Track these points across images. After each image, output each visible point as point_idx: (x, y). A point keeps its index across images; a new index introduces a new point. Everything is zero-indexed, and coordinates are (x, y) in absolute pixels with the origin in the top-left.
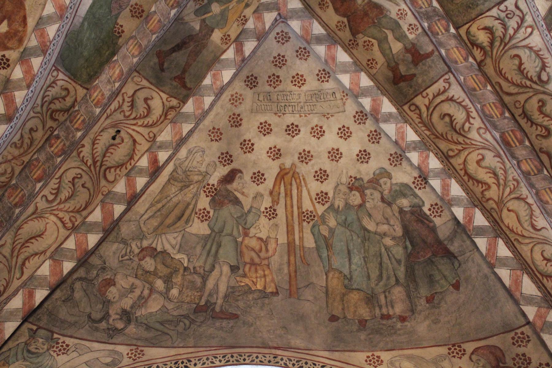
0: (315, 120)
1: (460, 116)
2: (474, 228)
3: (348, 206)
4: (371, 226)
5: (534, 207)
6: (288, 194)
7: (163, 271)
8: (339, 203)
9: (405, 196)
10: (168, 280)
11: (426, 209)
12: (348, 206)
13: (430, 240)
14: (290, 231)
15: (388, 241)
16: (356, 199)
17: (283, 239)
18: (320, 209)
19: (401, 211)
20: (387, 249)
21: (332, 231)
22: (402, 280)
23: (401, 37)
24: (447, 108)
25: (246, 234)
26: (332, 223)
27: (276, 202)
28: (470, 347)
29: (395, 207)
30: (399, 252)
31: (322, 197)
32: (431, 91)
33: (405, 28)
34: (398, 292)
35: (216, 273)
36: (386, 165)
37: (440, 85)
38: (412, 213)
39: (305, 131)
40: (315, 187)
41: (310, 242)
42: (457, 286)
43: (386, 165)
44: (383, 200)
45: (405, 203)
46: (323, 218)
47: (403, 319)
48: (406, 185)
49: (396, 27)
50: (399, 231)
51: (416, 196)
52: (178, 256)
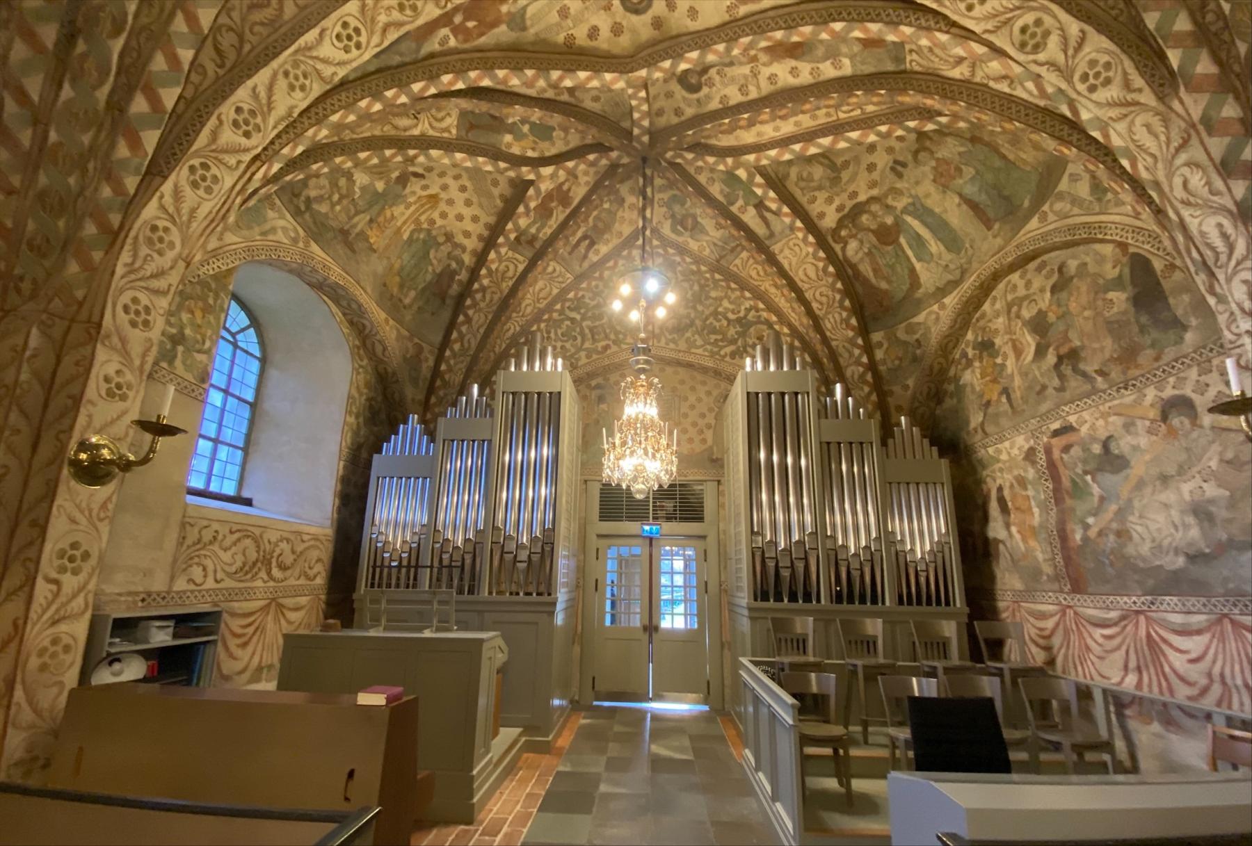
0: (475, 200)
1: (510, 274)
3: (435, 238)
4: (431, 256)
6: (422, 206)
7: (344, 191)
8: (434, 233)
10: (342, 197)
11: (457, 278)
12: (435, 238)
14: (405, 223)
15: (430, 269)
16: (441, 239)
17: (399, 224)
18: (425, 226)
19: (449, 265)
20: (427, 271)
21: (418, 239)
23: (539, 230)
24: (512, 267)
25: (391, 206)
26: (422, 236)
27: (415, 203)
30: (429, 277)
31: (432, 222)
32: (517, 256)
34: (412, 294)
35: (362, 216)
36: (469, 250)
37: (521, 258)
39: (466, 195)
40: (436, 215)
41: (405, 237)
42: (433, 314)
43: (469, 250)
44: (449, 253)
45: (454, 265)
46: (421, 230)
47: (405, 307)
49: (543, 226)
50: (438, 271)
52: (357, 190)
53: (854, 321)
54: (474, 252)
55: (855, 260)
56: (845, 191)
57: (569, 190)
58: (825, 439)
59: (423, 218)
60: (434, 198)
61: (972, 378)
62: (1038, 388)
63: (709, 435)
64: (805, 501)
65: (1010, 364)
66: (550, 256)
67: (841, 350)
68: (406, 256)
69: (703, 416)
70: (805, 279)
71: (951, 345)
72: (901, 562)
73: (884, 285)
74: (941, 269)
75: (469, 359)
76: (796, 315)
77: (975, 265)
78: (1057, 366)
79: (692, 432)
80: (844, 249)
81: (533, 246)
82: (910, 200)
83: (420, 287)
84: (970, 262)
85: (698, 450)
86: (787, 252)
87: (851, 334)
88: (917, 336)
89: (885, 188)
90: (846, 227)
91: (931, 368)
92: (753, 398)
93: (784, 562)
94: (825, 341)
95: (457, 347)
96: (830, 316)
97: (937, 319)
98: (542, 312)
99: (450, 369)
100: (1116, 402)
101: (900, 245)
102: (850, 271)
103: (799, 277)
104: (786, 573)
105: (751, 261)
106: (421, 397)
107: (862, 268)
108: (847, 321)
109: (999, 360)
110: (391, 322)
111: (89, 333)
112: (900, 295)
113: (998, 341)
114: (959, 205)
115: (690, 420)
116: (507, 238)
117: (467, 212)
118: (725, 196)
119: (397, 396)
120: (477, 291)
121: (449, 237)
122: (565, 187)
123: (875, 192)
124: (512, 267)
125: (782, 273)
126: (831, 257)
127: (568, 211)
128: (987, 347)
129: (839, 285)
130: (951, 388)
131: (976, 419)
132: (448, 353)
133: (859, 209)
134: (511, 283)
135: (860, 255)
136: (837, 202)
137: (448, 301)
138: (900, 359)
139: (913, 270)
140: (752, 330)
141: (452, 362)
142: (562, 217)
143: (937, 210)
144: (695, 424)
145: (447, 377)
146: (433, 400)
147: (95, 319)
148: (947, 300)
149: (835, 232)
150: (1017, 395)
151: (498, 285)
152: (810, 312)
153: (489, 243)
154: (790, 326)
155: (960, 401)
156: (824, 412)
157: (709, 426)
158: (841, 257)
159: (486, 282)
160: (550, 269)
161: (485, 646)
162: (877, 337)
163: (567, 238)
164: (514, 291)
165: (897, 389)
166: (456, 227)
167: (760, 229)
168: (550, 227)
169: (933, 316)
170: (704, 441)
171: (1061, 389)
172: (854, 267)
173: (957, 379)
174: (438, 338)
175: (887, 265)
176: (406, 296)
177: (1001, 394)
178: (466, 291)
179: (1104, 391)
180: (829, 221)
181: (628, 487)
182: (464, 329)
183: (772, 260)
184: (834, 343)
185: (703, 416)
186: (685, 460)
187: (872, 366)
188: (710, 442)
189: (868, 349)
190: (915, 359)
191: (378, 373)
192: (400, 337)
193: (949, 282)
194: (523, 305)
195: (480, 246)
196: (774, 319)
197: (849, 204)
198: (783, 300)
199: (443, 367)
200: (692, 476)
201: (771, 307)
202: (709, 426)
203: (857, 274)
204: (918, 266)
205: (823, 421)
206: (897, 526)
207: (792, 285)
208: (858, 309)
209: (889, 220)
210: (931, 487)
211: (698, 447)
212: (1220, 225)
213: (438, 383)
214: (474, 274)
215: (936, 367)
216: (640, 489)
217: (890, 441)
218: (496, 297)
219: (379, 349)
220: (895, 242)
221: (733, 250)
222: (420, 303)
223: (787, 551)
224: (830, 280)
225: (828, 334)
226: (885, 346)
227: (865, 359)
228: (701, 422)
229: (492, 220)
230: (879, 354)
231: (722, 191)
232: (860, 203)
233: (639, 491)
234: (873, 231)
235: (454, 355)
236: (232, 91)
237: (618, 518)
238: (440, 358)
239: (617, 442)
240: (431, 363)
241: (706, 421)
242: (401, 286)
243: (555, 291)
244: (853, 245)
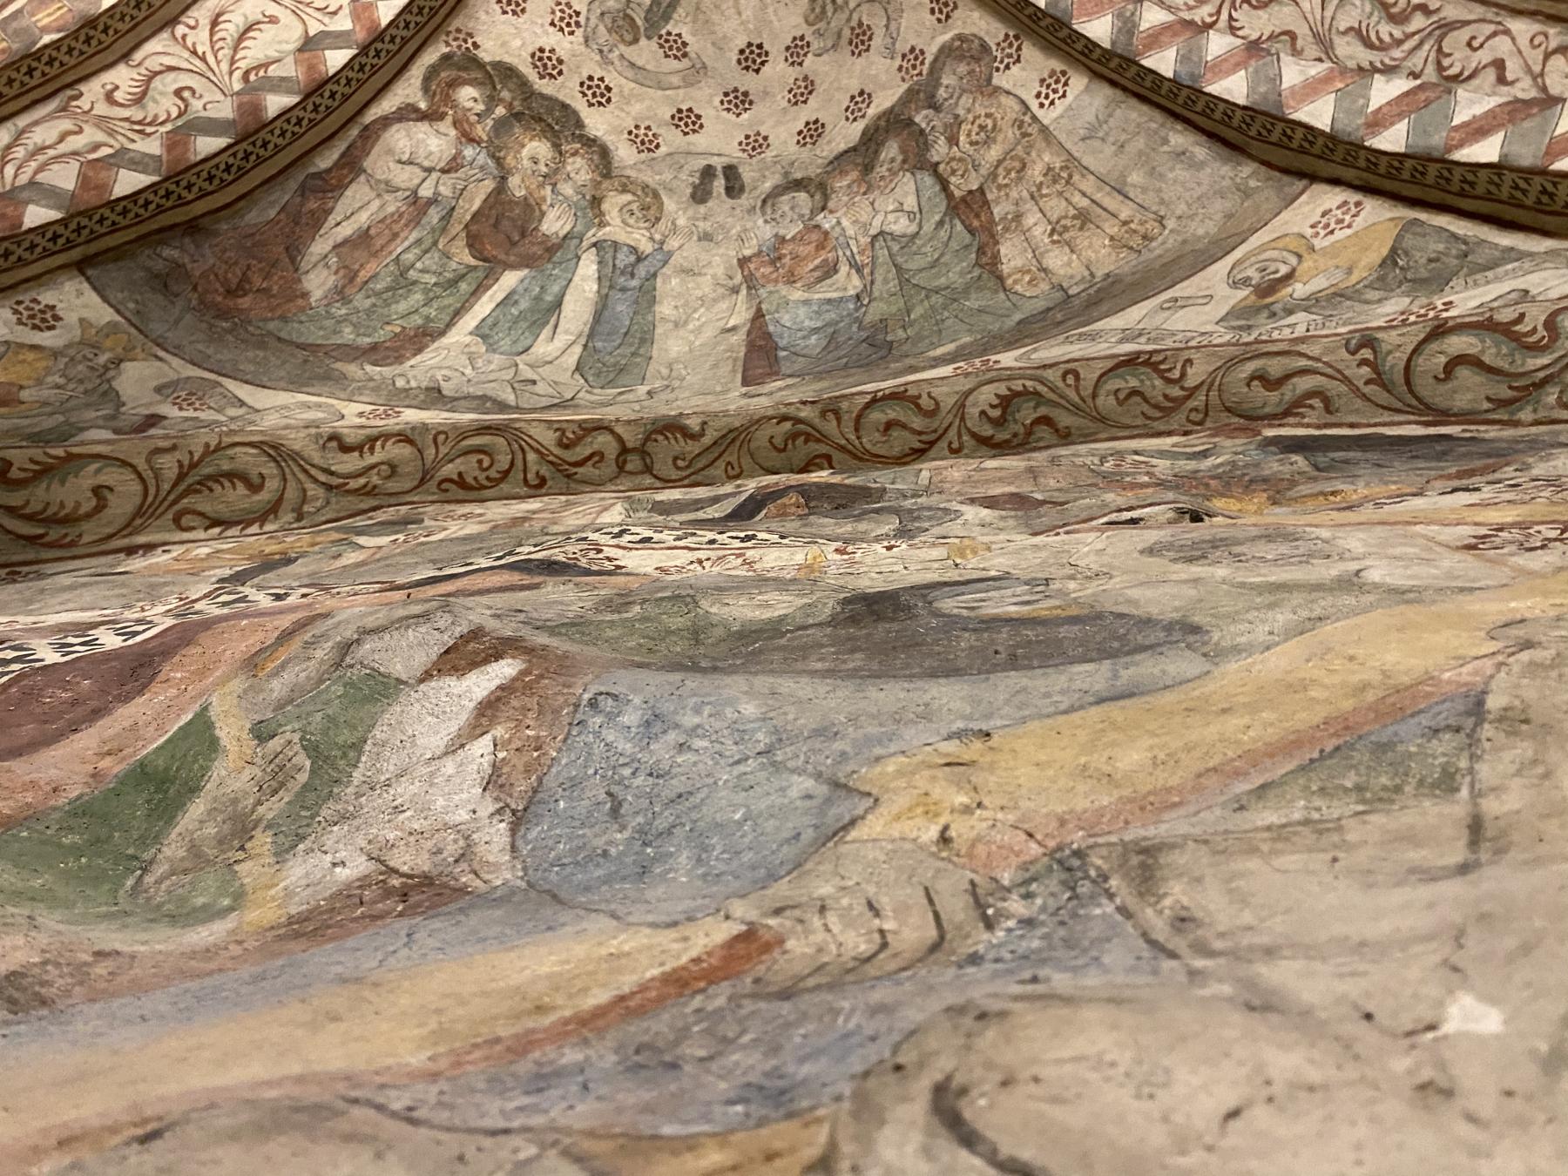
55: (378, 163)
70: (229, 29)
73: (318, 283)
80: (408, 113)
82: (646, 247)
90: (492, 101)
102: (325, 161)
107: (357, 193)
123: (624, 154)
135: (405, 177)
136: (564, 45)
149: (467, 65)
158: (374, 113)
172: (351, 165)
197: (566, 90)
203: (331, 185)
209: (555, 223)
220: (492, 268)
232: (579, 124)
244: (434, 142)
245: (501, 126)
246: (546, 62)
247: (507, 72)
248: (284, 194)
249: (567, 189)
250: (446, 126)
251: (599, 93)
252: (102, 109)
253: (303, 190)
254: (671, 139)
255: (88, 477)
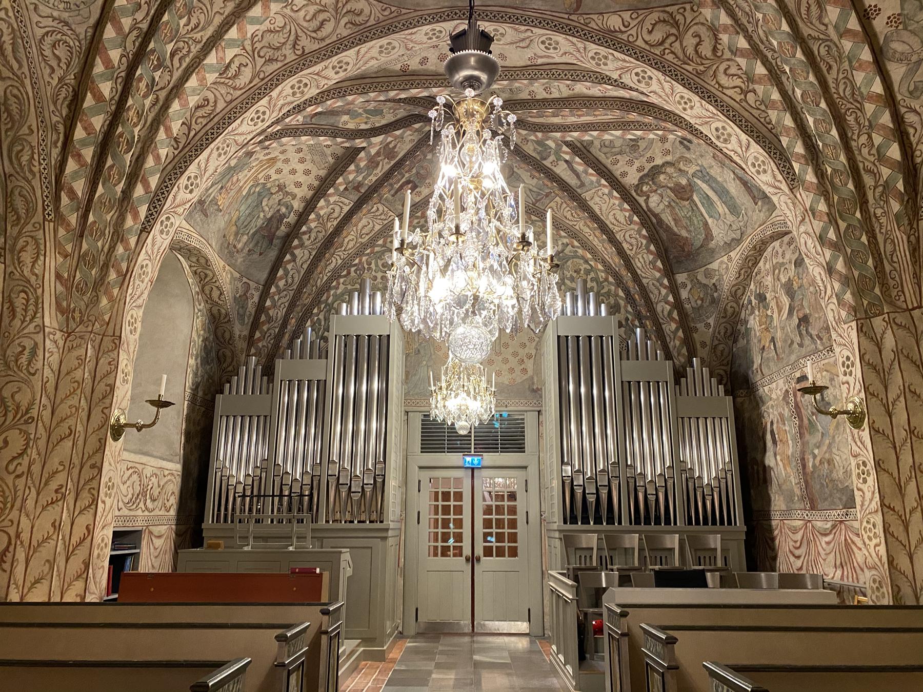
0: (308, 157)
1: (336, 215)
2: (293, 252)
4: (264, 204)
5: (310, 260)
8: (269, 185)
9: (287, 208)
11: (285, 220)
13: (273, 230)
15: (262, 215)
19: (278, 211)
20: (258, 217)
22: (250, 234)
23: (365, 179)
24: (337, 209)
26: (257, 190)
28: (245, 280)
29: (279, 207)
30: (260, 222)
33: (370, 178)
36: (298, 197)
37: (347, 201)
38: (280, 215)
40: (272, 172)
45: (284, 210)
46: (258, 184)
48: (293, 208)
50: (269, 216)
51: (290, 213)
53: (659, 264)
54: (303, 199)
55: (657, 210)
56: (643, 156)
57: (395, 146)
58: (625, 379)
59: (260, 176)
60: (274, 160)
61: (754, 322)
62: (789, 342)
63: (529, 365)
64: (609, 431)
65: (775, 316)
66: (375, 200)
67: (652, 287)
68: (243, 208)
69: (524, 345)
70: (615, 222)
71: (740, 292)
72: (691, 485)
73: (684, 233)
74: (727, 228)
75: (292, 293)
76: (609, 253)
77: (749, 231)
78: (799, 326)
79: (513, 362)
80: (646, 201)
81: (359, 191)
82: (698, 168)
83: (251, 232)
84: (746, 226)
85: (519, 380)
86: (597, 199)
87: (658, 275)
88: (714, 281)
89: (678, 155)
90: (647, 184)
91: (725, 310)
92: (563, 341)
93: (591, 489)
94: (636, 278)
95: (281, 283)
96: (640, 256)
97: (727, 268)
98: (364, 246)
99: (274, 306)
100: (826, 361)
101: (693, 201)
102: (654, 220)
103: (609, 220)
104: (592, 499)
105: (564, 205)
106: (246, 333)
107: (663, 217)
108: (653, 263)
109: (769, 313)
110: (227, 268)
111: (115, 343)
112: (698, 244)
113: (768, 296)
114: (734, 179)
115: (511, 350)
116: (337, 189)
117: (300, 168)
118: (538, 153)
119: (227, 335)
120: (305, 233)
121: (281, 188)
122: (391, 146)
123: (669, 158)
124: (337, 209)
125: (594, 217)
126: (636, 208)
127: (393, 163)
128: (762, 298)
129: (644, 232)
130: (743, 329)
131: (757, 361)
132: (273, 289)
133: (655, 172)
134: (335, 223)
135: (662, 206)
136: (637, 164)
137: (276, 241)
138: (702, 300)
139: (706, 224)
140: (569, 263)
141: (276, 298)
142: (387, 167)
143: (719, 179)
144: (515, 354)
145: (271, 312)
146: (258, 335)
147: (117, 334)
148: (732, 254)
149: (638, 187)
150: (779, 344)
151: (323, 225)
152: (621, 252)
153: (320, 192)
154: (604, 262)
155: (748, 341)
156: (625, 352)
157: (529, 357)
158: (645, 208)
159: (313, 225)
160: (375, 209)
161: (342, 556)
162: (681, 278)
163: (391, 185)
164: (338, 230)
165: (700, 326)
166: (289, 181)
167: (572, 181)
168: (376, 175)
169: (724, 266)
170: (524, 371)
171: (801, 345)
172: (656, 216)
173: (746, 322)
174: (263, 276)
175: (685, 217)
176: (239, 241)
177: (770, 342)
178: (294, 231)
179: (821, 351)
180: (632, 178)
181: (453, 424)
182: (289, 267)
183: (584, 206)
184: (644, 281)
185: (524, 345)
186: (501, 392)
187: (678, 304)
188: (530, 373)
189: (674, 289)
190: (713, 301)
191: (212, 315)
192: (233, 278)
193: (733, 239)
194: (346, 240)
195: (311, 193)
196: (589, 256)
197: (648, 167)
198: (597, 240)
199: (268, 303)
200: (514, 407)
201: (585, 245)
202: (529, 357)
203: (660, 221)
204: (710, 221)
205: (624, 362)
206: (688, 455)
207: (604, 228)
208: (663, 253)
209: (684, 182)
210: (717, 421)
211: (519, 378)
212: (820, 274)
213: (263, 318)
214: (302, 218)
215: (730, 311)
216: (462, 427)
217: (683, 380)
218: (321, 236)
219: (215, 294)
220: (690, 198)
221: (547, 196)
222: (251, 246)
223: (594, 479)
224: (636, 227)
225: (639, 272)
226: (689, 287)
227: (671, 299)
228: (522, 352)
229: (323, 173)
230: (684, 294)
231: (535, 149)
232: (658, 166)
233: (462, 428)
234: (670, 189)
235: (279, 291)
236: (187, 167)
237: (439, 449)
238: (265, 294)
239: (444, 385)
240: (256, 299)
241: (526, 350)
242: (236, 234)
243: (377, 227)
244: (654, 200)
245: (653, 183)
246: (639, 170)
247: (641, 178)
248: (661, 231)
249: (675, 175)
250: (651, 195)
251: (651, 159)
252: (633, 252)
253: (661, 227)
254: (667, 146)
255: (728, 307)
